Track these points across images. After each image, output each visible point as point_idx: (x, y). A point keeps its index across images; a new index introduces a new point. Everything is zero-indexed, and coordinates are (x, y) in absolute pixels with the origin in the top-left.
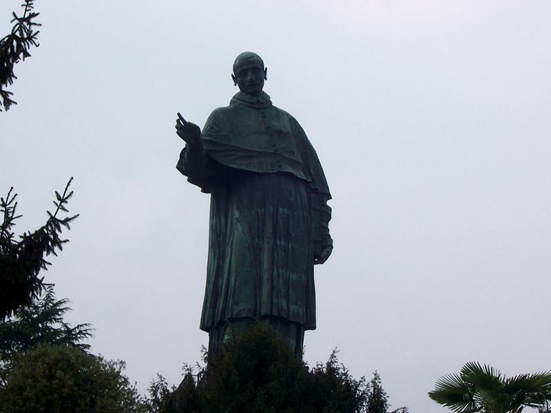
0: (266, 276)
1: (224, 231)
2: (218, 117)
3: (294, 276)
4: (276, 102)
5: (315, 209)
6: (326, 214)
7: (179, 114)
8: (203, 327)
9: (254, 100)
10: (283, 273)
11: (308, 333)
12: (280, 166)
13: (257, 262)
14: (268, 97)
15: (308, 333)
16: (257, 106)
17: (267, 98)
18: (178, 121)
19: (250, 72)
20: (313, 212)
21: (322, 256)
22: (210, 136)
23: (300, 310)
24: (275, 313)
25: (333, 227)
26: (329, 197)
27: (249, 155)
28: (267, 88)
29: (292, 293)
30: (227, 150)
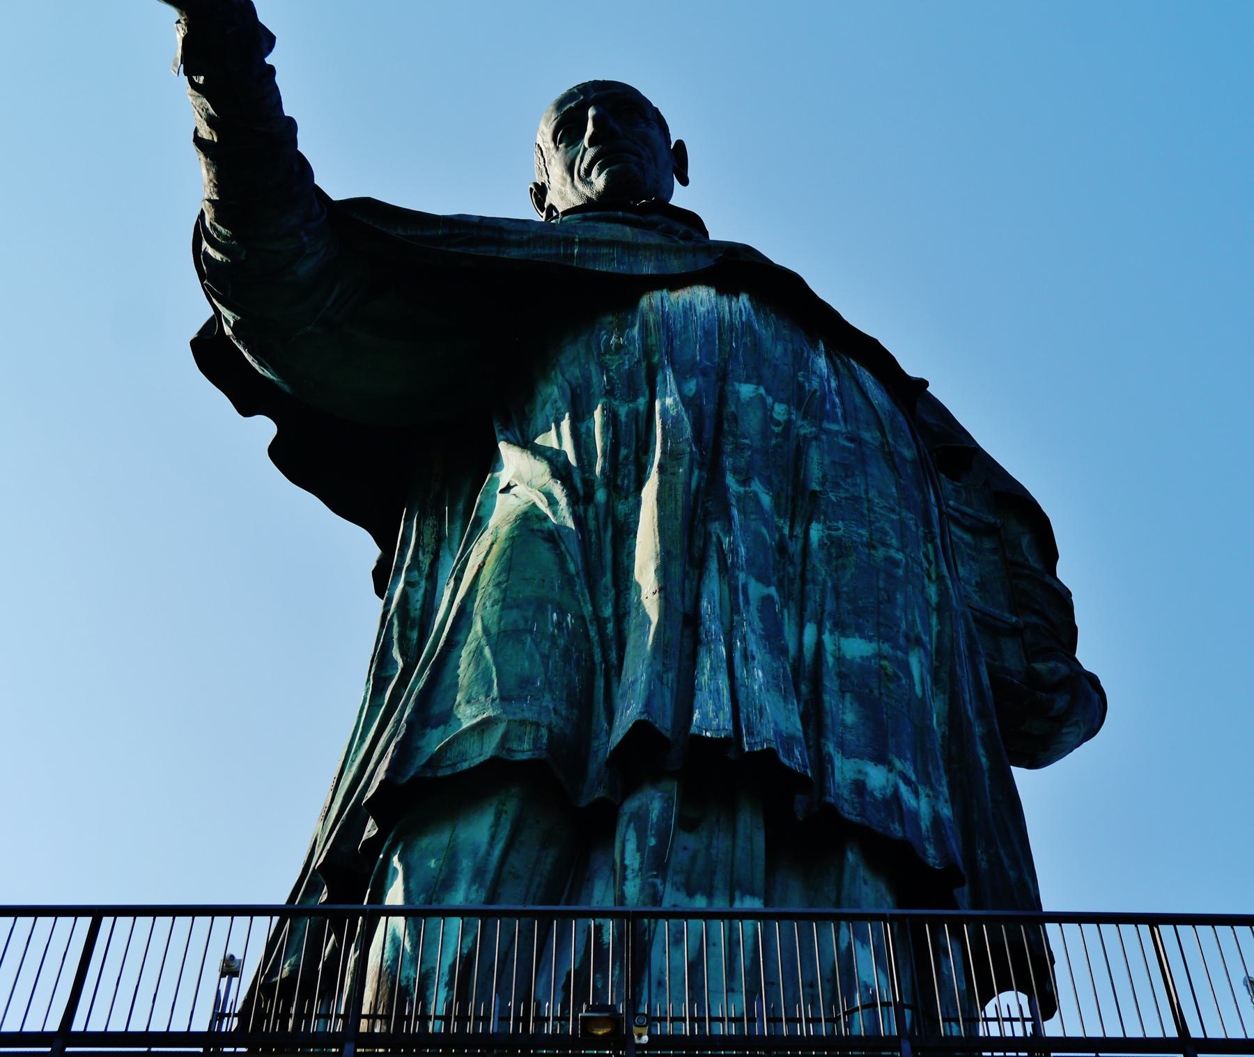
3: (857, 648)
10: (767, 601)
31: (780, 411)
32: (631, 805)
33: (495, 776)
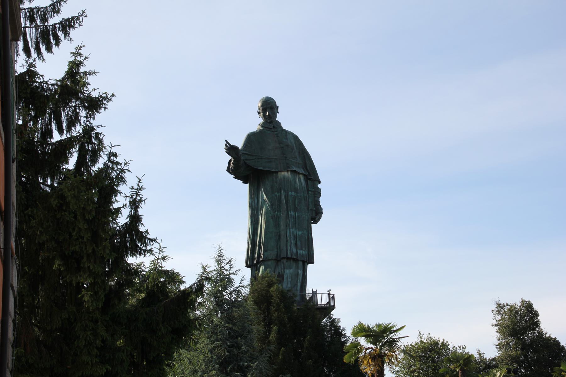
0: (283, 233)
1: (256, 206)
2: (251, 138)
3: (300, 233)
4: (285, 127)
5: (311, 191)
6: (318, 193)
7: (226, 141)
8: (247, 266)
9: (271, 126)
11: (309, 266)
12: (288, 167)
13: (277, 225)
14: (280, 123)
15: (309, 266)
16: (273, 130)
17: (279, 124)
18: (226, 145)
19: (269, 108)
20: (310, 192)
21: (316, 219)
22: (246, 151)
23: (304, 253)
24: (289, 255)
25: (323, 201)
26: (320, 182)
28: (279, 118)
29: (299, 243)
31: (293, 193)
32: (282, 261)
33: (272, 259)
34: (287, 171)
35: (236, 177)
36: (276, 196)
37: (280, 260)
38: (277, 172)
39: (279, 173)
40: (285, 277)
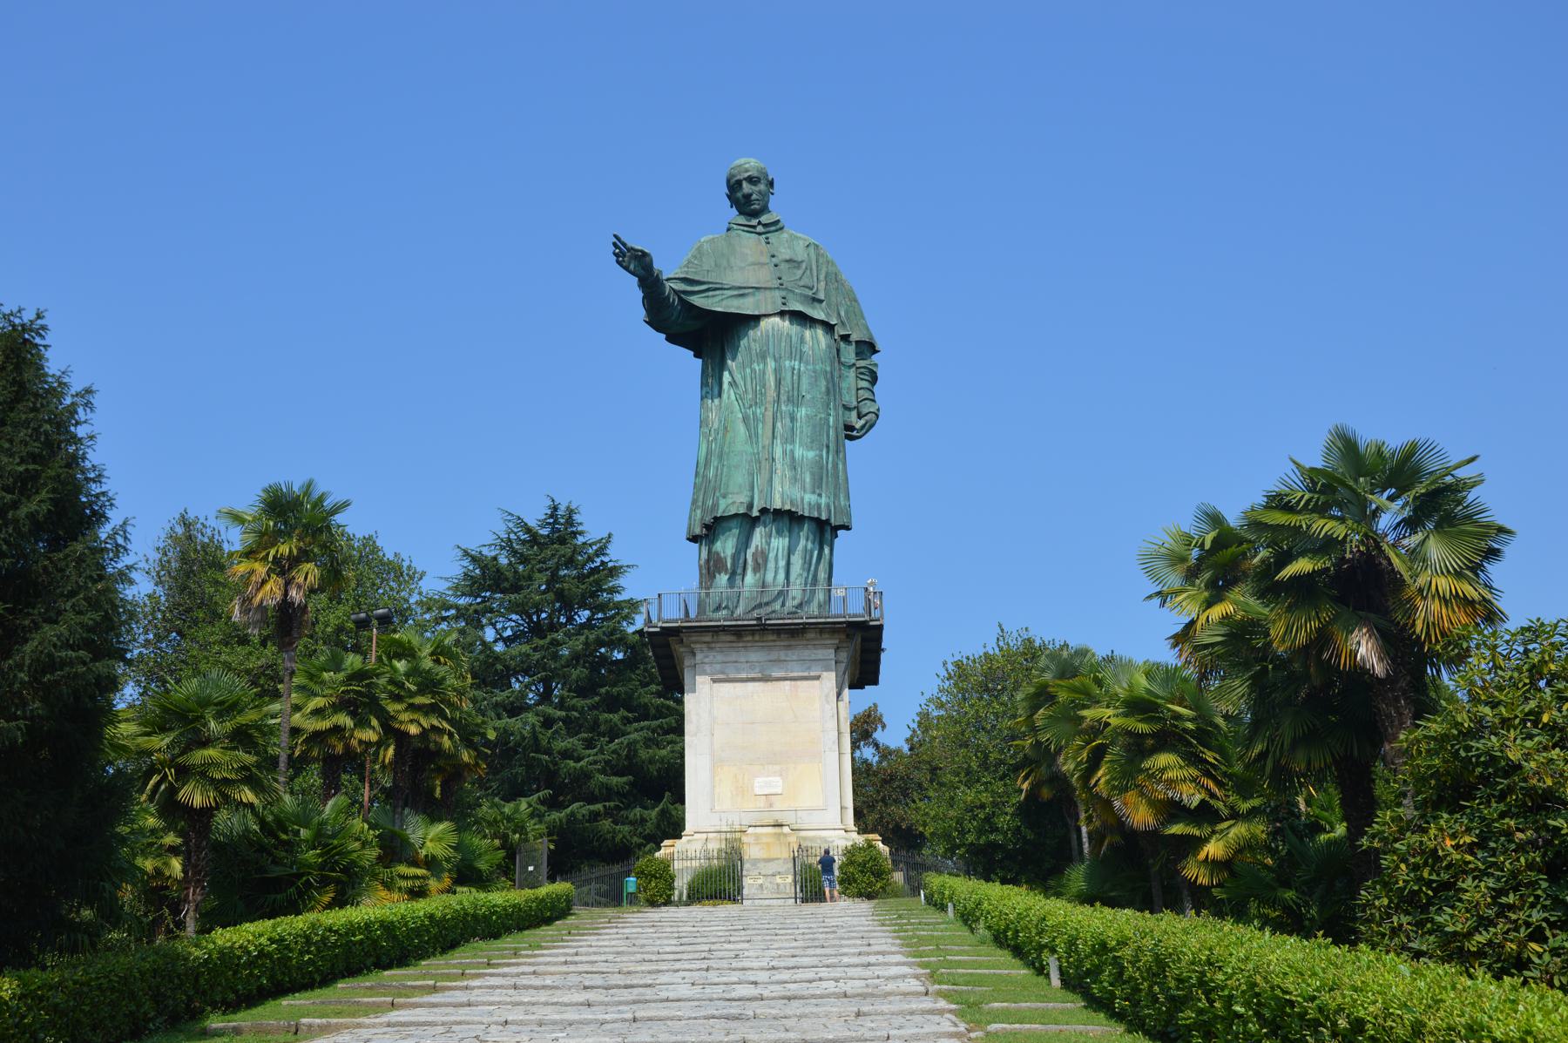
3: (811, 454)
24: (777, 505)
27: (742, 291)
30: (708, 290)
33: (736, 515)
34: (782, 314)
35: (672, 339)
36: (753, 371)
37: (754, 522)
38: (755, 319)
39: (764, 323)
40: (772, 556)
